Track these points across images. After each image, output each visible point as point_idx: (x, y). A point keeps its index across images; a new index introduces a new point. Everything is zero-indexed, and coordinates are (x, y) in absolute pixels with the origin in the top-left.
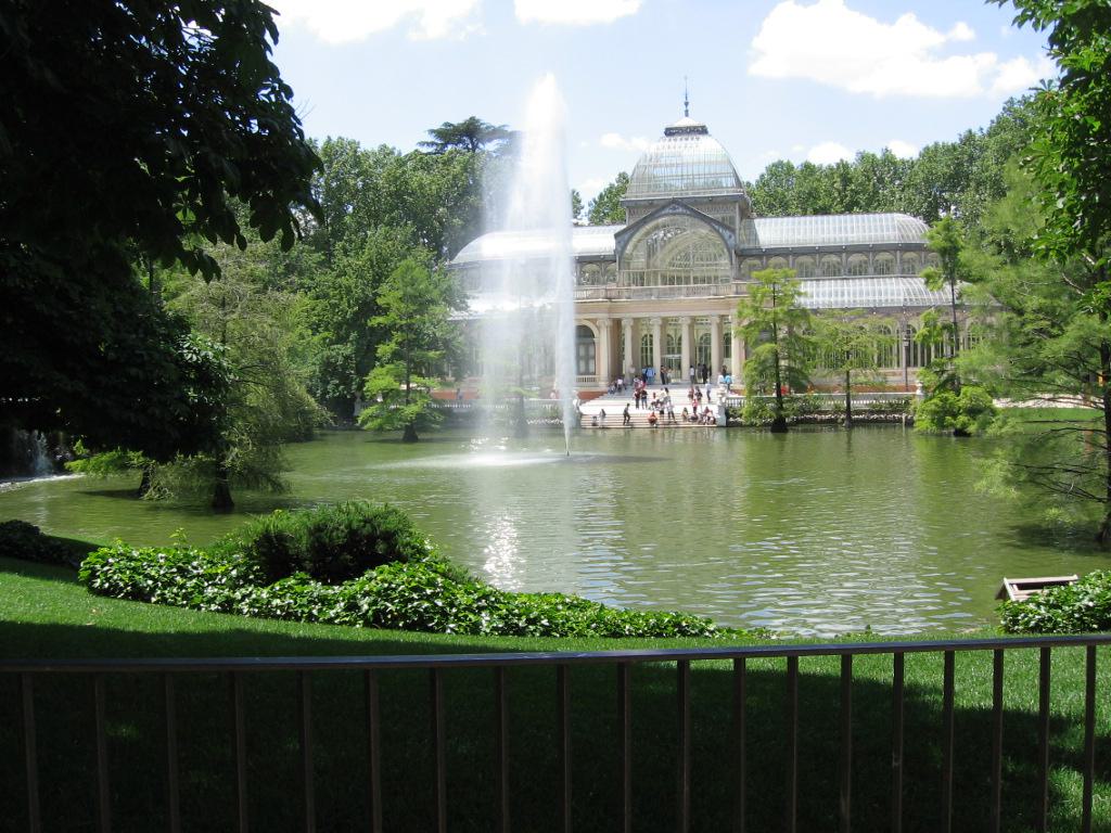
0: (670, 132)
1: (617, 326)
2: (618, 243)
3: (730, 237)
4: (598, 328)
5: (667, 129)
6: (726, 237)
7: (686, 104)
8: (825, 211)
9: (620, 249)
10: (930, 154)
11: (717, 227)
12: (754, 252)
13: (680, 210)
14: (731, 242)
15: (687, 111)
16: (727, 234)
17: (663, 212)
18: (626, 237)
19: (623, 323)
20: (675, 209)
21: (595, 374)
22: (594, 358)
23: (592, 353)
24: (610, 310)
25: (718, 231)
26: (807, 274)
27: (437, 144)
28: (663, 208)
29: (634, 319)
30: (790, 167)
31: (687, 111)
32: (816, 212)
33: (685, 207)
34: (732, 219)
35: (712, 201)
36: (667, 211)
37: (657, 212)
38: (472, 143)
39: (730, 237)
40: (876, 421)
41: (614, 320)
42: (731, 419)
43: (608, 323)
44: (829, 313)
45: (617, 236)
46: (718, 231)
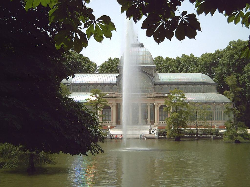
2: (117, 79)
3: (153, 79)
4: (113, 106)
6: (152, 79)
8: (174, 72)
9: (118, 81)
10: (206, 56)
11: (149, 75)
12: (159, 84)
14: (153, 80)
16: (152, 78)
21: (111, 121)
23: (110, 114)
24: (116, 100)
25: (149, 77)
26: (188, 91)
30: (162, 58)
32: (171, 72)
39: (153, 79)
40: (203, 137)
42: (160, 136)
43: (116, 104)
44: (192, 103)
46: (149, 77)
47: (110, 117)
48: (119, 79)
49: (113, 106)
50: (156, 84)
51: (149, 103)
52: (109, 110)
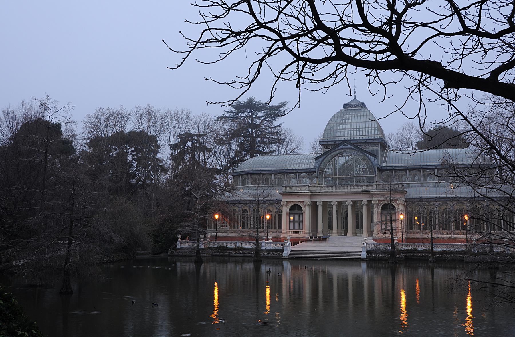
0: (345, 106)
1: (314, 206)
3: (374, 160)
4: (305, 205)
9: (317, 166)
11: (368, 155)
12: (388, 168)
13: (349, 146)
16: (373, 158)
17: (340, 147)
18: (321, 159)
20: (346, 145)
21: (302, 229)
22: (302, 221)
23: (301, 219)
27: (234, 113)
28: (340, 145)
29: (323, 201)
33: (352, 144)
34: (377, 151)
35: (366, 142)
36: (342, 147)
37: (334, 148)
38: (252, 112)
39: (374, 160)
45: (316, 159)
46: (368, 157)
47: (301, 224)
48: (319, 163)
49: (305, 205)
50: (381, 170)
51: (364, 199)
52: (299, 212)
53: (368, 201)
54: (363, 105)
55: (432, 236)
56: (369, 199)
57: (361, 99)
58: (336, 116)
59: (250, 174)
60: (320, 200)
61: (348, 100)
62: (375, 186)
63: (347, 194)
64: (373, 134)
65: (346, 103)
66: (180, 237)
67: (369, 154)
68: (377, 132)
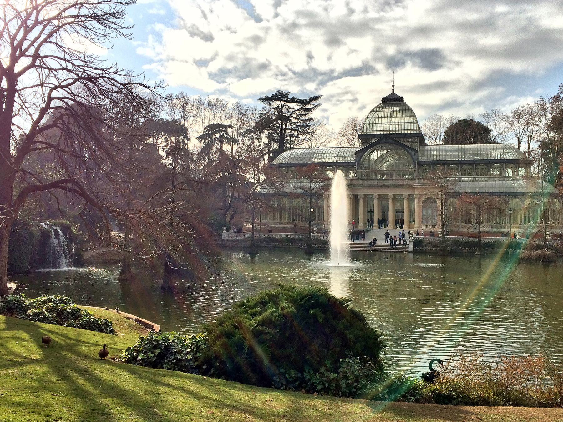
0: (385, 100)
3: (415, 155)
5: (383, 98)
7: (393, 86)
11: (408, 149)
15: (393, 90)
16: (413, 153)
19: (359, 197)
31: (393, 90)
33: (392, 139)
35: (406, 136)
39: (415, 155)
41: (353, 195)
50: (420, 164)
53: (409, 195)
54: (401, 99)
55: (479, 230)
56: (410, 193)
57: (398, 93)
58: (375, 110)
59: (288, 166)
60: (361, 193)
61: (387, 93)
62: (417, 181)
63: (388, 187)
64: (409, 128)
65: (385, 96)
66: (225, 228)
67: (410, 149)
68: (415, 127)
